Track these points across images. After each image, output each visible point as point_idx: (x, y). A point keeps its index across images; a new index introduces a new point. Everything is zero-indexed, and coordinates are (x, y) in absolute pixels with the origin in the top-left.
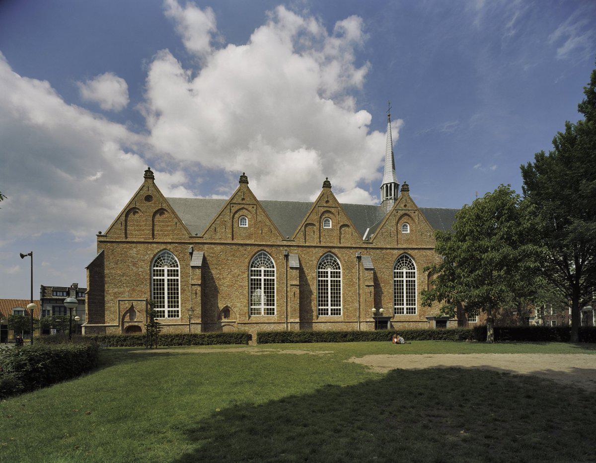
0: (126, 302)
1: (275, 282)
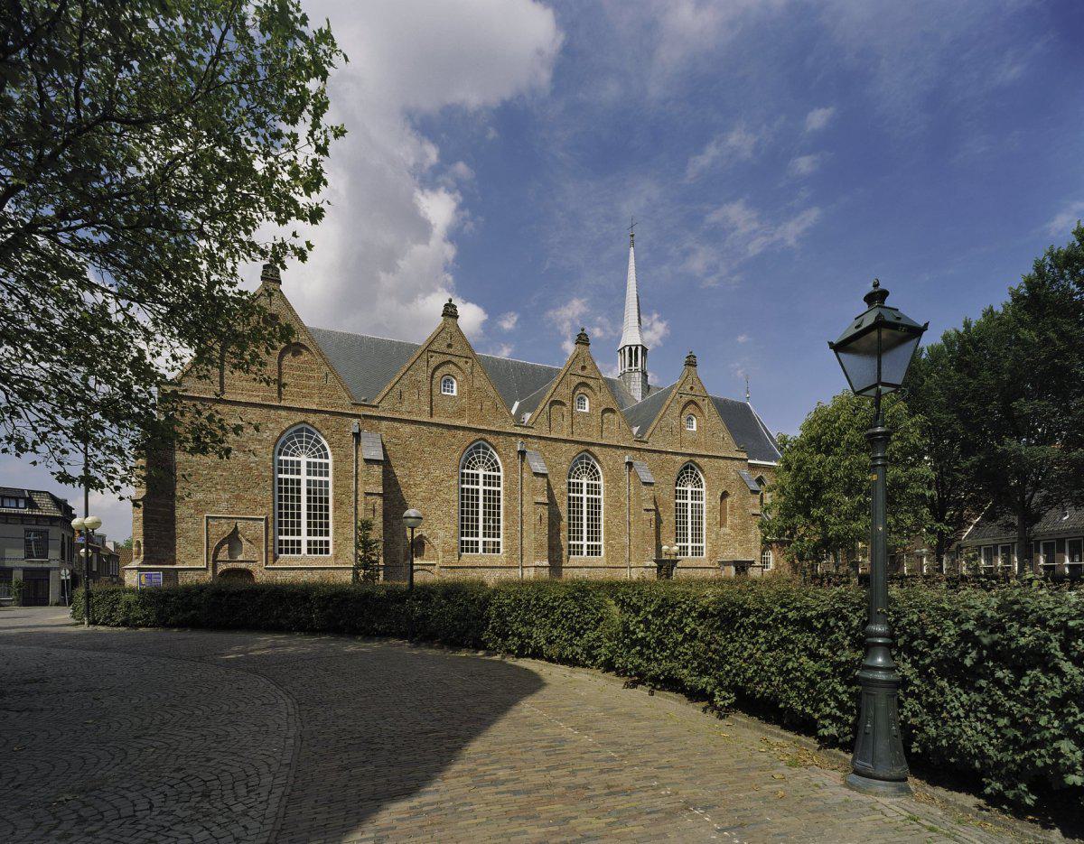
0: (223, 521)
1: (502, 497)
